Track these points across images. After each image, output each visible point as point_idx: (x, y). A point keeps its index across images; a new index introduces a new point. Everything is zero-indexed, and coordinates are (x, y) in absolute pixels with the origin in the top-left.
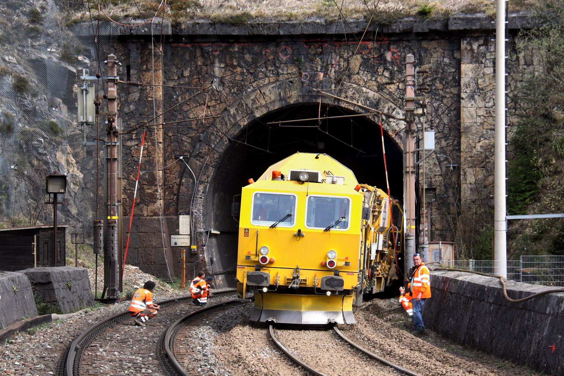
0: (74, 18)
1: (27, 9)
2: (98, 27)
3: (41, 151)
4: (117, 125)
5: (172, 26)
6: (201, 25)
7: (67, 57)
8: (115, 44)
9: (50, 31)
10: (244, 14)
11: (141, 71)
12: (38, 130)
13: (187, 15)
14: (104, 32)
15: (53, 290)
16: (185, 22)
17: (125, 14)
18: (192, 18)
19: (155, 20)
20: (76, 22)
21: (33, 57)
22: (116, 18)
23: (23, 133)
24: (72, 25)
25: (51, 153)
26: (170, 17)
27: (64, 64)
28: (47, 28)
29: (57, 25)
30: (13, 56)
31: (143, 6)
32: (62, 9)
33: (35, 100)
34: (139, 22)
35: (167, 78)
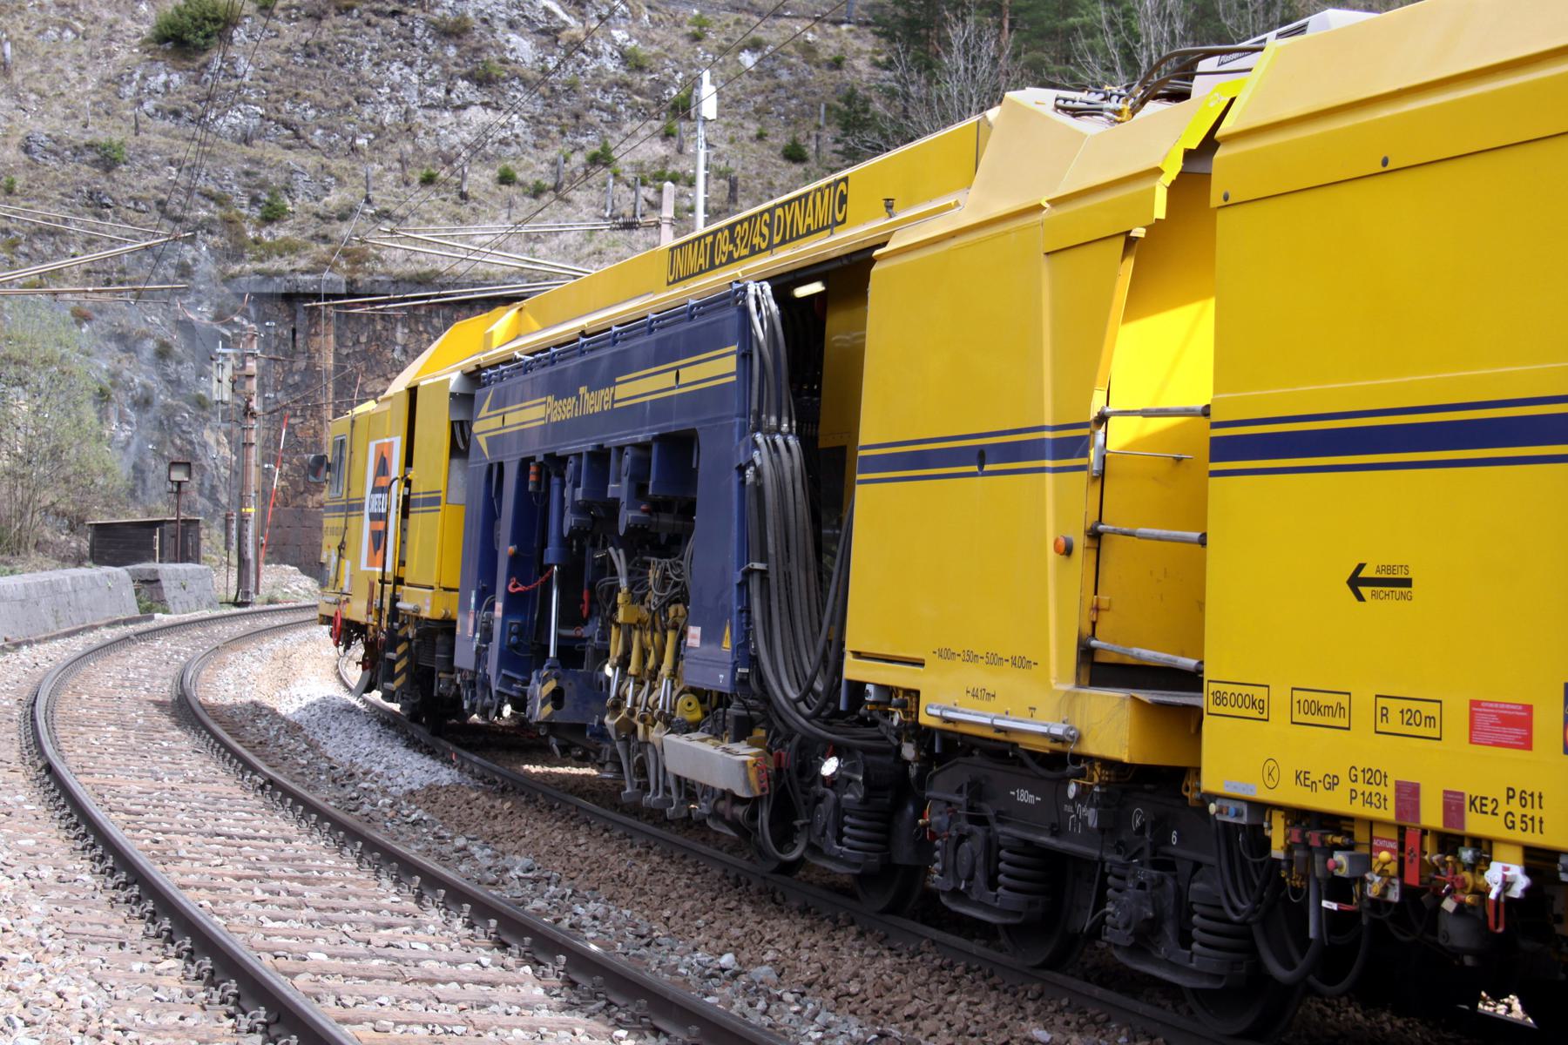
0: (231, 271)
1: (175, 261)
2: (260, 283)
3: (184, 428)
4: (255, 405)
5: (347, 283)
6: (381, 283)
7: (219, 317)
8: (279, 304)
9: (202, 287)
10: (433, 271)
11: (308, 335)
12: (182, 403)
13: (365, 271)
14: (269, 288)
15: (161, 588)
16: (363, 279)
17: (292, 267)
18: (371, 274)
19: (326, 276)
20: (233, 277)
21: (181, 318)
22: (279, 273)
23: (165, 407)
24: (229, 279)
25: (196, 431)
26: (345, 272)
27: (217, 326)
28: (199, 283)
29: (211, 280)
30: (156, 316)
31: (314, 259)
32: (217, 261)
33: (180, 368)
34: (308, 277)
35: (340, 343)
